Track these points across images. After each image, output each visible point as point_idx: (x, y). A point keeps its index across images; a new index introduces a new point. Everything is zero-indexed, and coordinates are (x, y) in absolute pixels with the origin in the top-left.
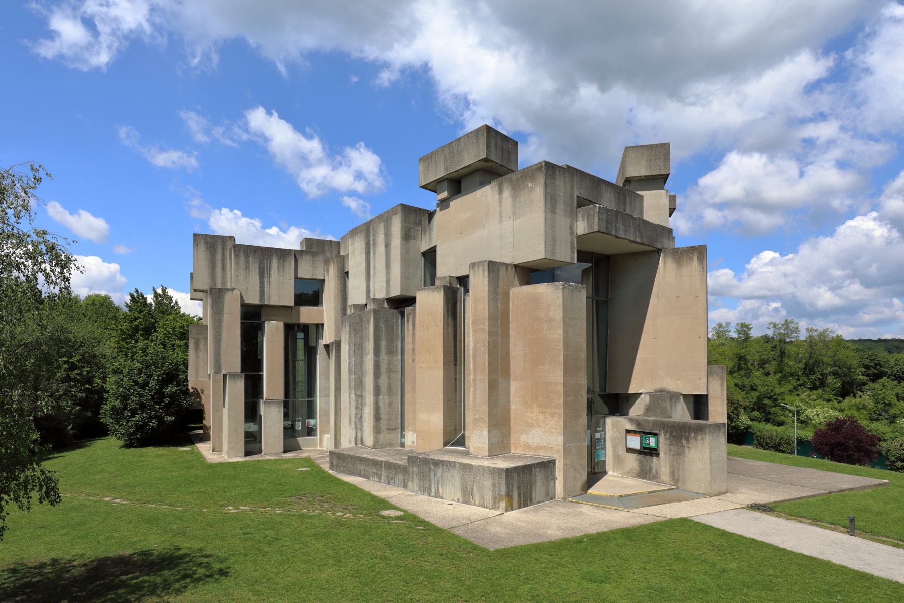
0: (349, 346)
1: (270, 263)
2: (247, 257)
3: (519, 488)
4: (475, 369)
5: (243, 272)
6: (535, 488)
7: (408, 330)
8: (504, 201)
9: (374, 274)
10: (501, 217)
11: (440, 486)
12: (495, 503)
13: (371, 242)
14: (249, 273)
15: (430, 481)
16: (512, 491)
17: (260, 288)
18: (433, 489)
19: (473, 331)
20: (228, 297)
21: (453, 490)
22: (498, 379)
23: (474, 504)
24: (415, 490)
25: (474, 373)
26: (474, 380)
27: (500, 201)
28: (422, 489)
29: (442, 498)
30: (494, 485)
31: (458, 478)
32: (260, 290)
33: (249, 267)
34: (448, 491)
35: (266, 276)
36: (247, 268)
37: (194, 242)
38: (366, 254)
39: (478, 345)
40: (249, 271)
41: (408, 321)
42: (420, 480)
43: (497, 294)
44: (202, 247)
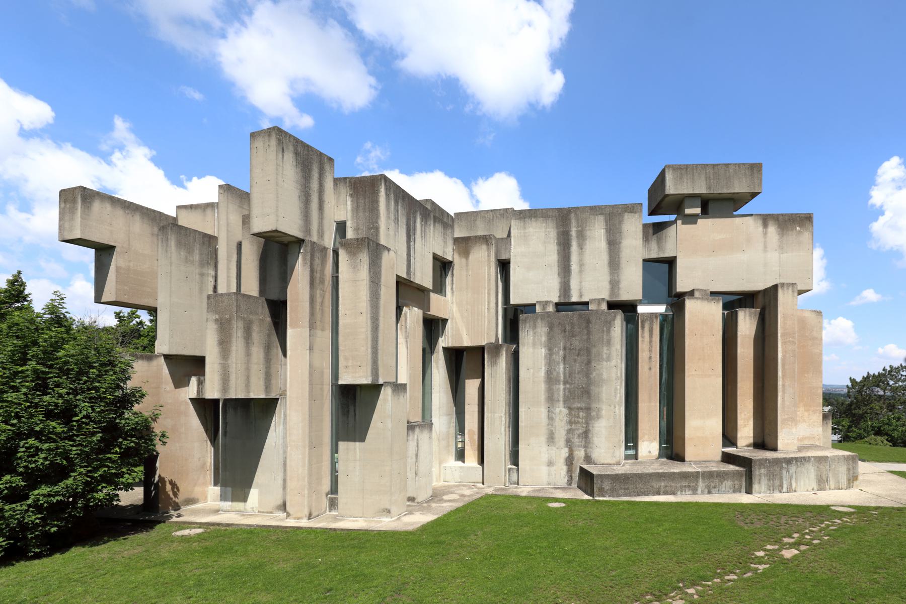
0: (550, 349)
1: (415, 222)
4: (784, 376)
7: (643, 337)
8: (769, 235)
9: (581, 271)
10: (765, 247)
11: (793, 481)
12: (849, 483)
13: (573, 233)
14: (398, 228)
15: (781, 478)
18: (785, 486)
19: (782, 343)
21: (807, 481)
23: (830, 489)
24: (763, 490)
25: (783, 379)
26: (784, 386)
27: (765, 234)
28: (772, 489)
29: (795, 491)
30: (849, 470)
31: (813, 471)
34: (802, 483)
38: (559, 244)
39: (787, 355)
41: (643, 327)
42: (769, 480)
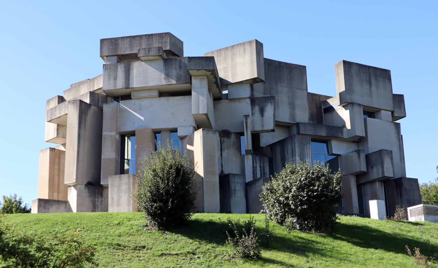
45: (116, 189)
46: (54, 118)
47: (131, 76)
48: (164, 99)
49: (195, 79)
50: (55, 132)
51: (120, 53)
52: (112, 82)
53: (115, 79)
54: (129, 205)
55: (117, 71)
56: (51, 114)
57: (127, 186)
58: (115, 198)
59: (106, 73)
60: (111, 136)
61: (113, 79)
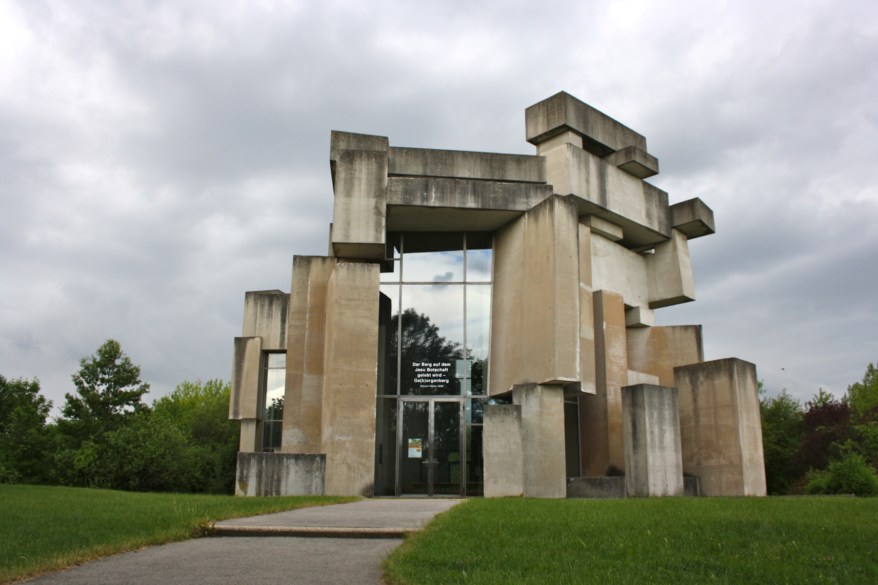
2: (271, 304)
3: (259, 475)
5: (265, 319)
6: (287, 478)
16: (247, 477)
17: (281, 334)
20: (250, 344)
22: (302, 375)
32: (281, 336)
33: (272, 315)
35: (287, 322)
36: (270, 316)
37: (246, 300)
40: (272, 318)
43: (307, 287)
44: (251, 303)
45: (656, 414)
46: (418, 202)
47: (607, 188)
48: (618, 248)
49: (678, 235)
50: (378, 231)
51: (590, 135)
52: (584, 184)
53: (588, 181)
54: (676, 451)
55: (589, 167)
56: (406, 192)
57: (671, 412)
58: (656, 431)
59: (575, 159)
60: (587, 293)
61: (586, 182)
